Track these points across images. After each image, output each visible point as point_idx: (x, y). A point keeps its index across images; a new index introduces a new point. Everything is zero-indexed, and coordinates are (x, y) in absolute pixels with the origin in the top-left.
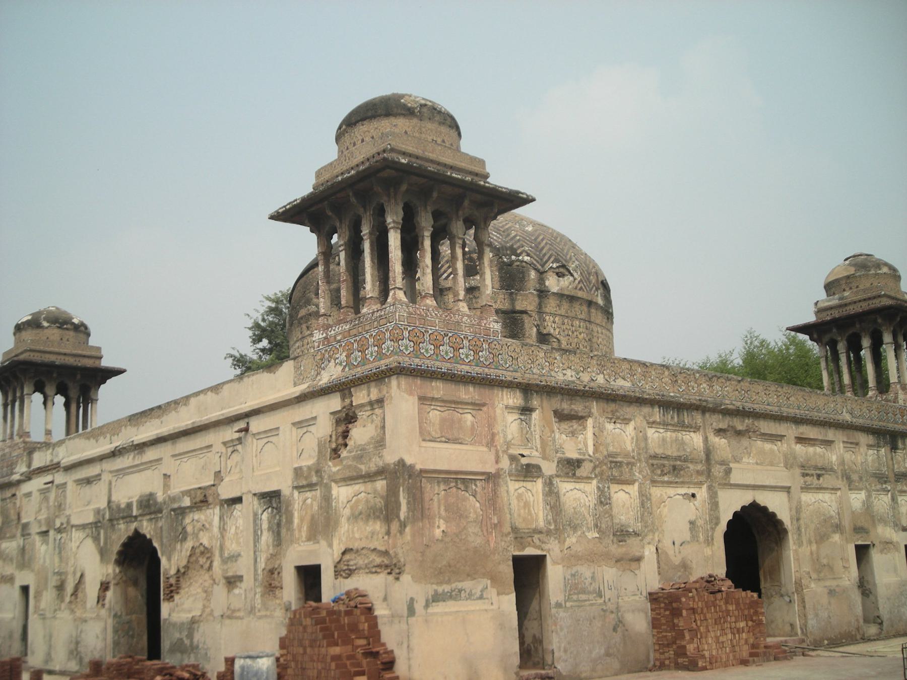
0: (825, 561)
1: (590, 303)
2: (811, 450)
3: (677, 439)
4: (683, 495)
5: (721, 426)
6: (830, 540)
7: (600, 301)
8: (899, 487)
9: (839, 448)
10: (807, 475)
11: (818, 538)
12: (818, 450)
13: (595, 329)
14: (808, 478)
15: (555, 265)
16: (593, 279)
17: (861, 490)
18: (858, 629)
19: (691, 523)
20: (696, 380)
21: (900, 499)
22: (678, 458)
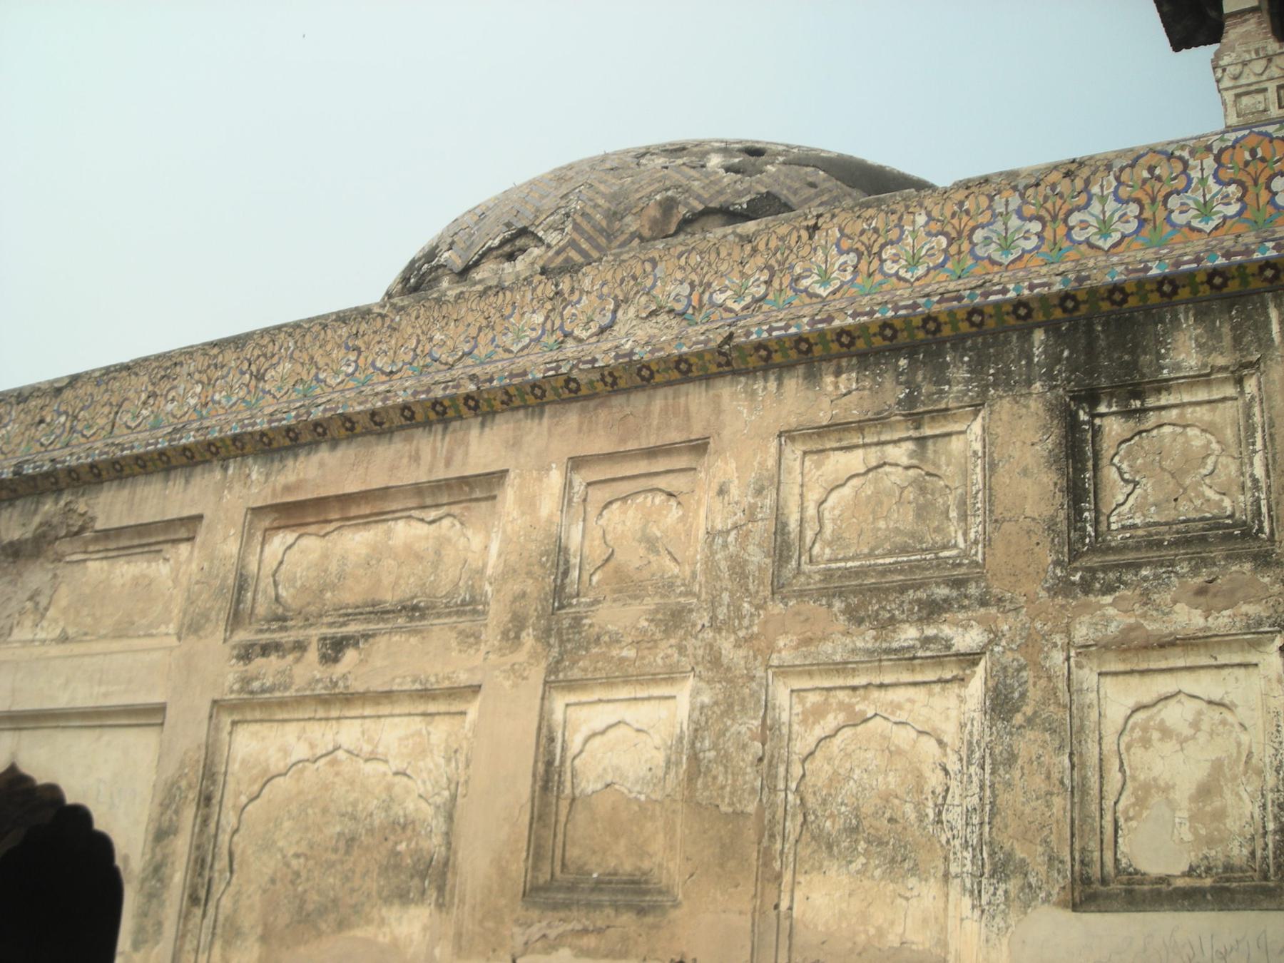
2: (355, 542)
6: (359, 933)
8: (1112, 614)
9: (529, 504)
10: (266, 650)
11: (283, 919)
12: (404, 532)
14: (259, 662)
15: (497, 242)
17: (671, 676)
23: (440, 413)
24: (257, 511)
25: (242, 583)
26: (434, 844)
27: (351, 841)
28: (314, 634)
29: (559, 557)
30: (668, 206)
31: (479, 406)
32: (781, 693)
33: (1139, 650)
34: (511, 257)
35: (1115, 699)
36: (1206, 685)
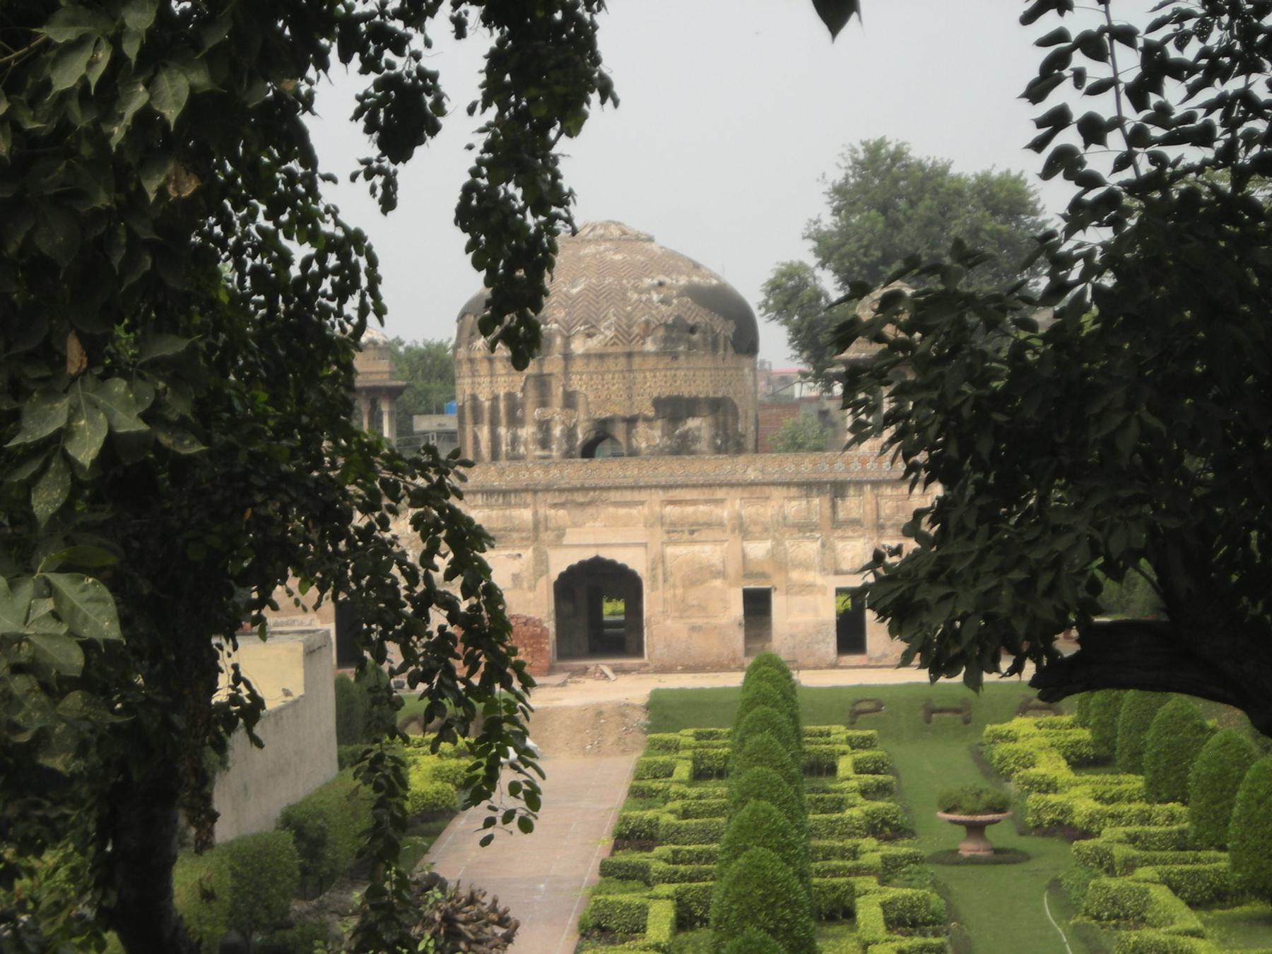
0: (694, 602)
1: (630, 355)
2: (690, 509)
3: (504, 516)
4: (509, 556)
5: (556, 501)
7: (650, 346)
8: (839, 533)
9: (733, 505)
12: (702, 508)
13: (640, 376)
16: (636, 330)
18: (734, 660)
19: (513, 575)
20: (527, 469)
21: (840, 545)
22: (505, 529)
23: (710, 486)
24: (663, 501)
25: (662, 517)
26: (721, 568)
27: (701, 568)
28: (686, 528)
29: (740, 517)
30: (647, 323)
31: (720, 485)
32: (787, 543)
33: (843, 538)
34: (590, 336)
35: (840, 545)
36: (853, 543)
